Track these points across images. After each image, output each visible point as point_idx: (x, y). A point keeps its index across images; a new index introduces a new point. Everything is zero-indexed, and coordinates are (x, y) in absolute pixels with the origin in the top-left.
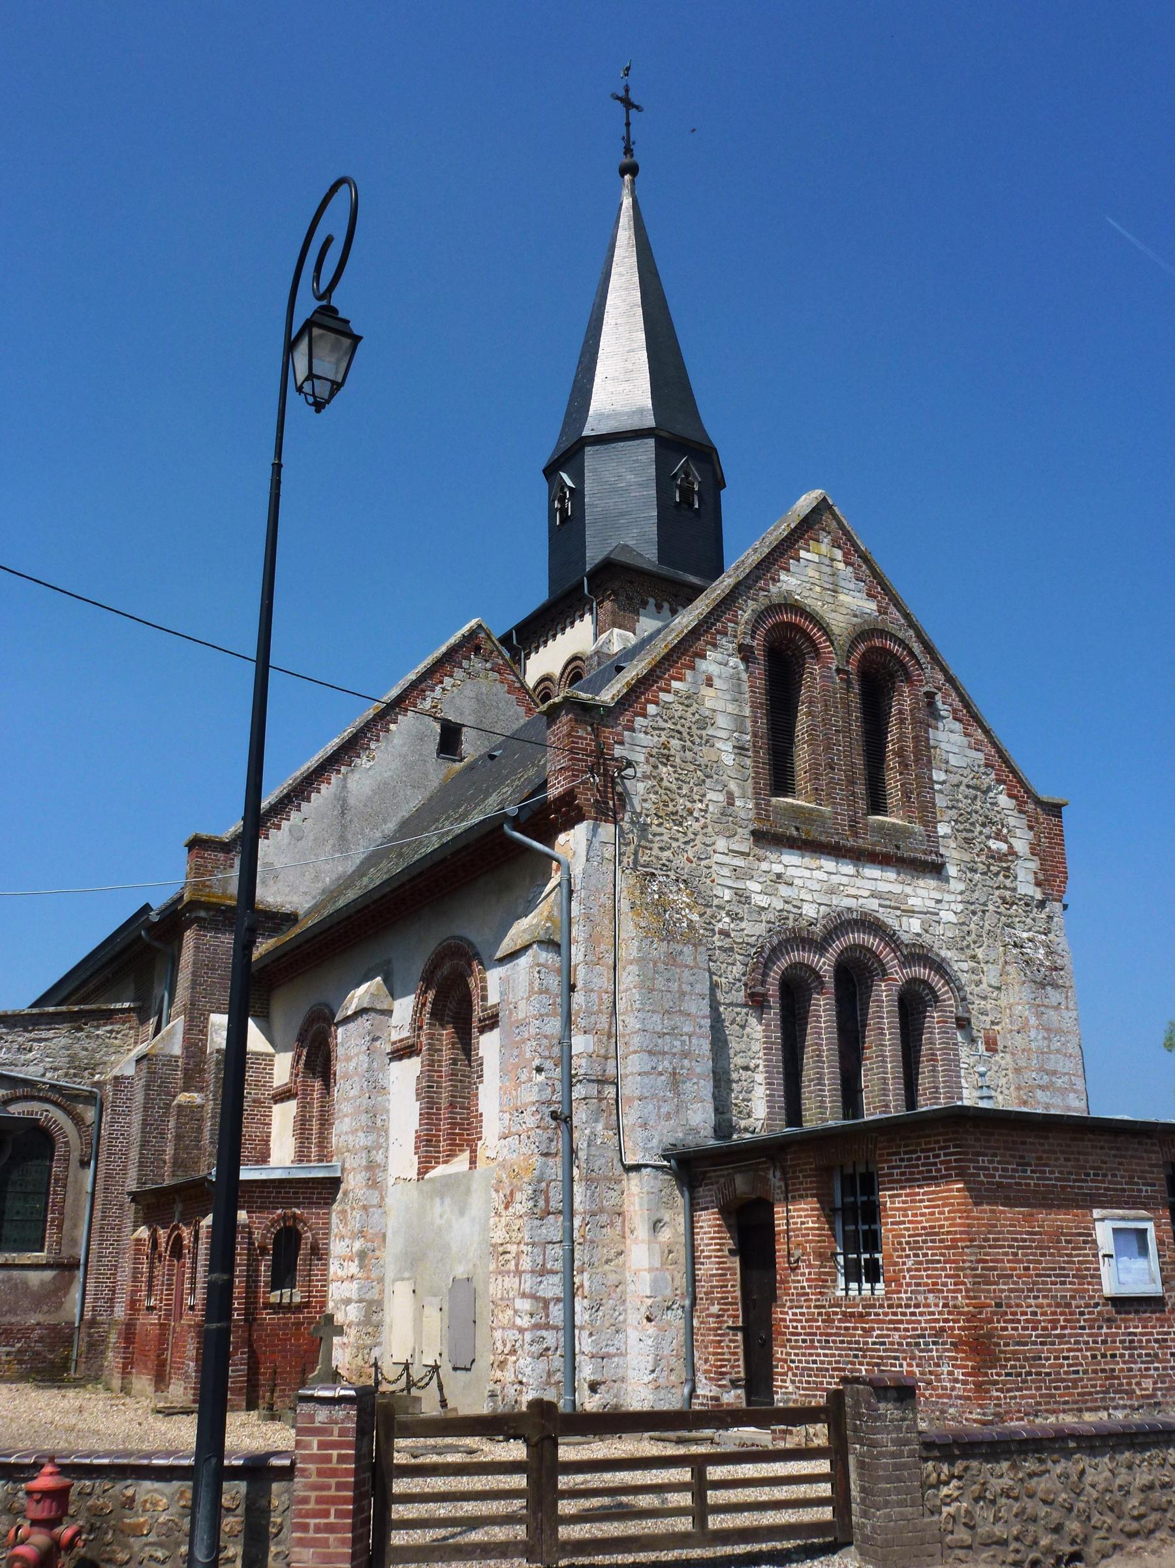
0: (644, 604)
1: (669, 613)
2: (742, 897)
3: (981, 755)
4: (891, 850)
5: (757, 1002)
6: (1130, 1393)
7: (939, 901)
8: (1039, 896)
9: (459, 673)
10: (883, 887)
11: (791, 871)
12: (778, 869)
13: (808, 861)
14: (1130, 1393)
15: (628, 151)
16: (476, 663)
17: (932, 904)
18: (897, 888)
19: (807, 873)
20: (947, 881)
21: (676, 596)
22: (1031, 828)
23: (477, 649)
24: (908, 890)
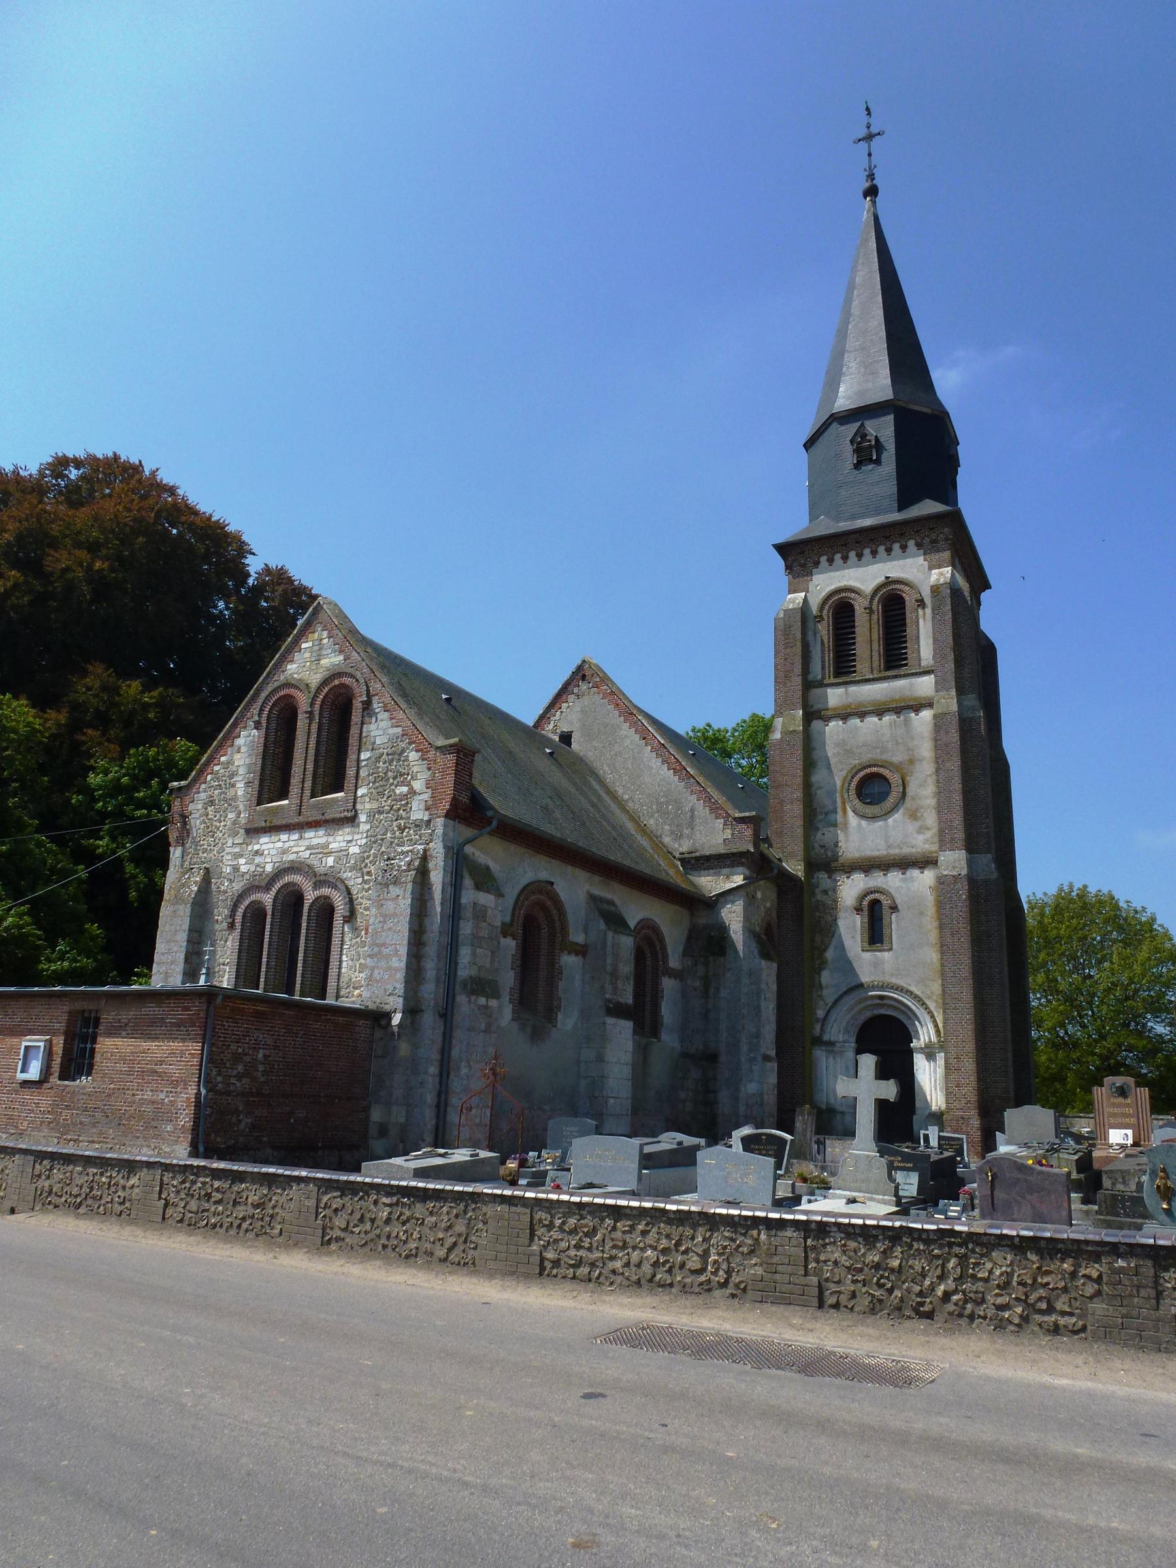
0: (817, 564)
1: (841, 561)
2: (236, 869)
3: (399, 730)
4: (319, 817)
5: (858, 910)
6: (17, 1127)
7: (349, 842)
8: (426, 818)
9: (571, 698)
10: (315, 841)
11: (264, 847)
12: (256, 847)
13: (274, 838)
14: (17, 1127)
15: (871, 176)
16: (584, 686)
17: (344, 844)
18: (322, 840)
19: (271, 845)
20: (358, 826)
21: (845, 545)
22: (429, 769)
23: (584, 677)
24: (331, 839)
